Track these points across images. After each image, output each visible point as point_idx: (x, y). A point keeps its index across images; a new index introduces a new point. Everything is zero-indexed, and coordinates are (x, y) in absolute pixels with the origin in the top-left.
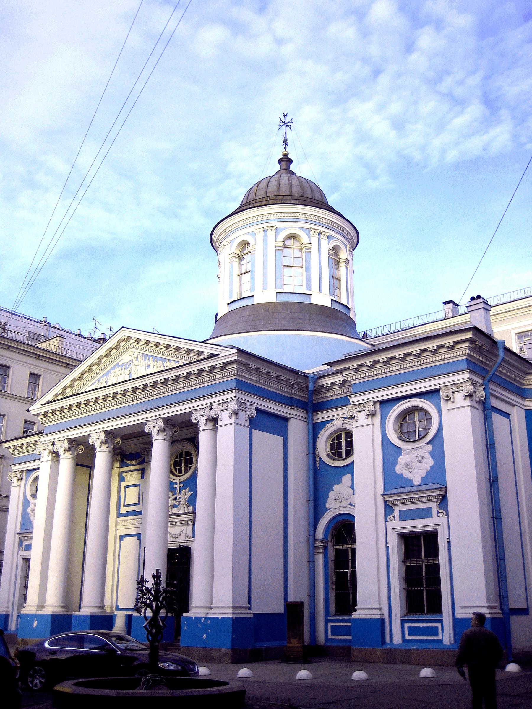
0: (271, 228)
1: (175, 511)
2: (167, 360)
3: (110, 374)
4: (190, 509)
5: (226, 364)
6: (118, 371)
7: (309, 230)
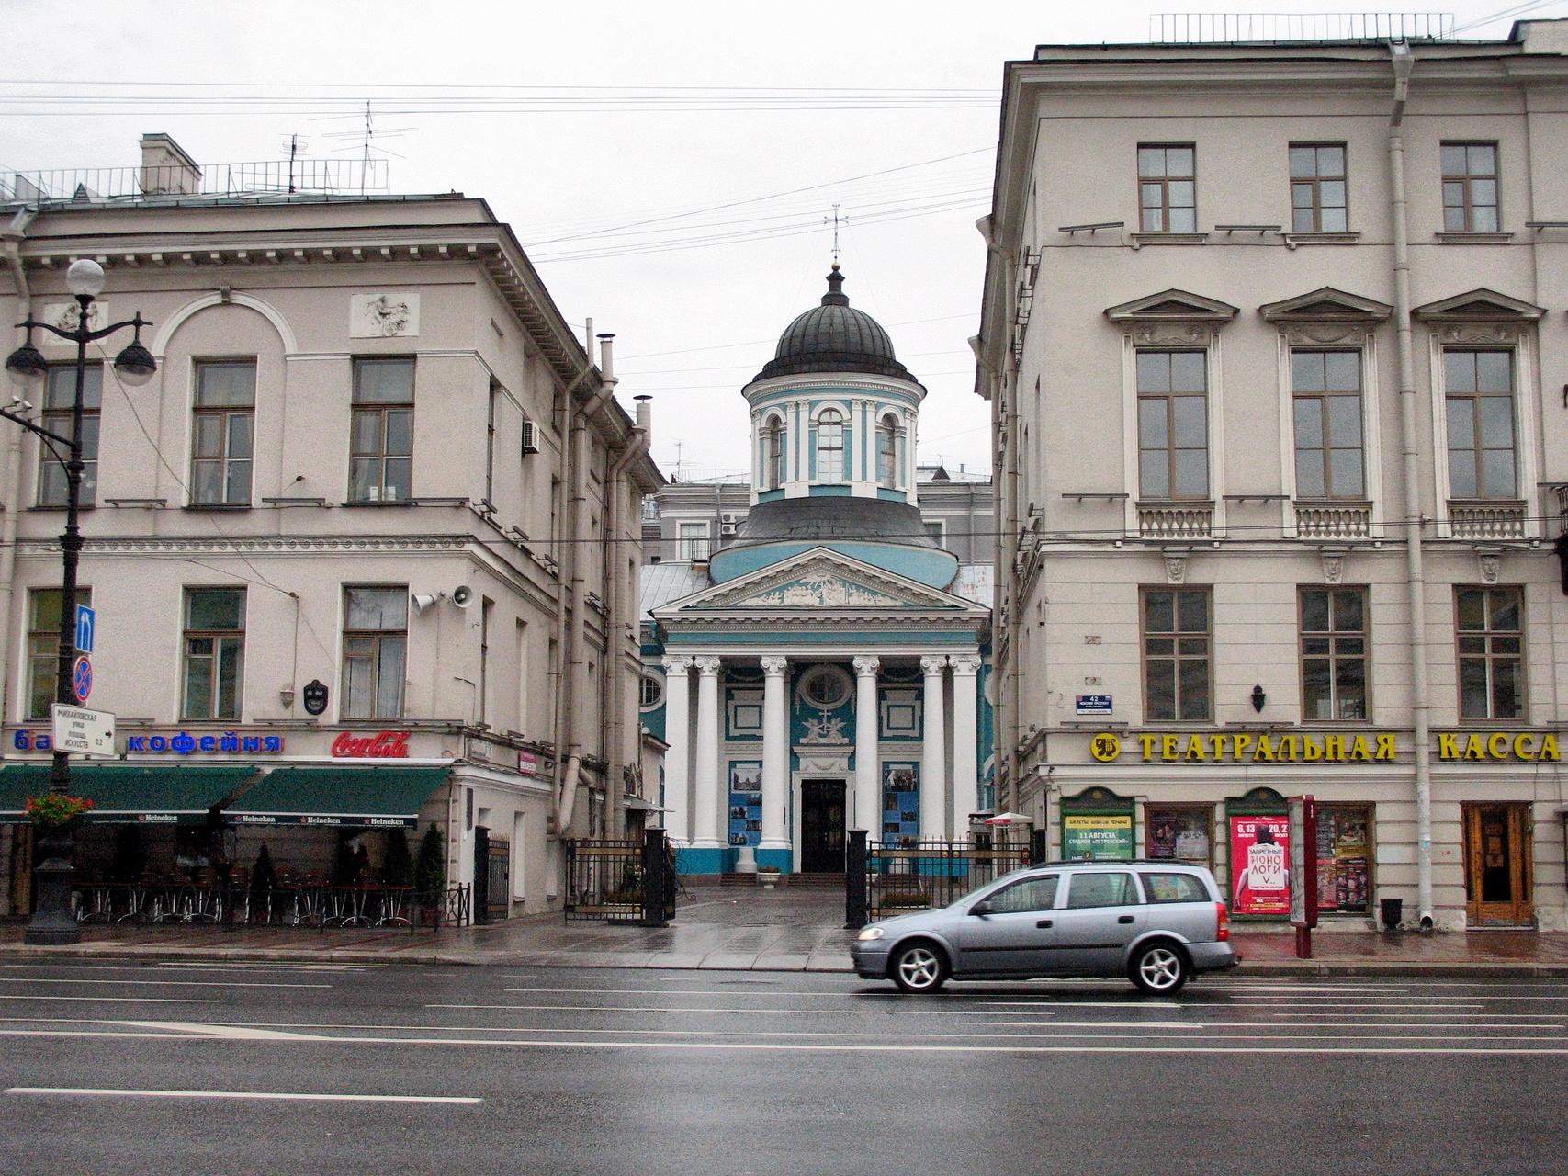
1: (822, 741)
4: (846, 740)
6: (797, 590)
7: (905, 410)
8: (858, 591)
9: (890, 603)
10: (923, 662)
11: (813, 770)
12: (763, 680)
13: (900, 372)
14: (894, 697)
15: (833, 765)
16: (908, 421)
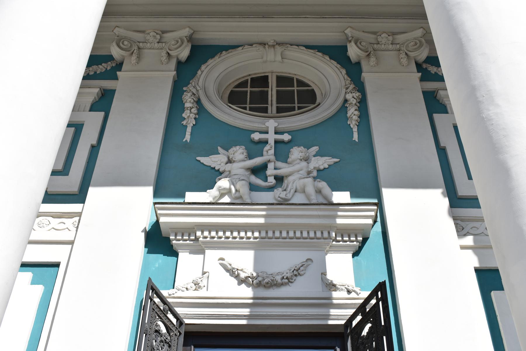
15: (297, 272)
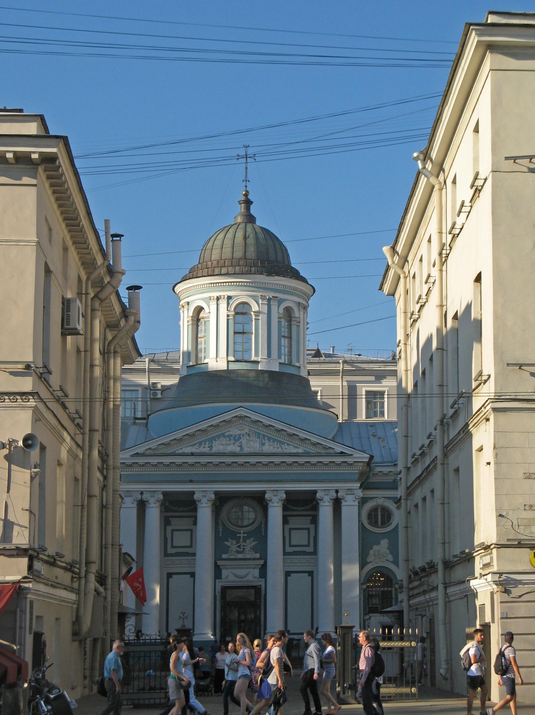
0: (274, 298)
1: (240, 556)
2: (286, 444)
3: (214, 441)
4: (258, 556)
5: (355, 462)
8: (269, 441)
9: (294, 451)
10: (318, 495)
11: (232, 578)
12: (195, 510)
13: (295, 275)
14: (294, 522)
15: (247, 575)
16: (302, 313)
